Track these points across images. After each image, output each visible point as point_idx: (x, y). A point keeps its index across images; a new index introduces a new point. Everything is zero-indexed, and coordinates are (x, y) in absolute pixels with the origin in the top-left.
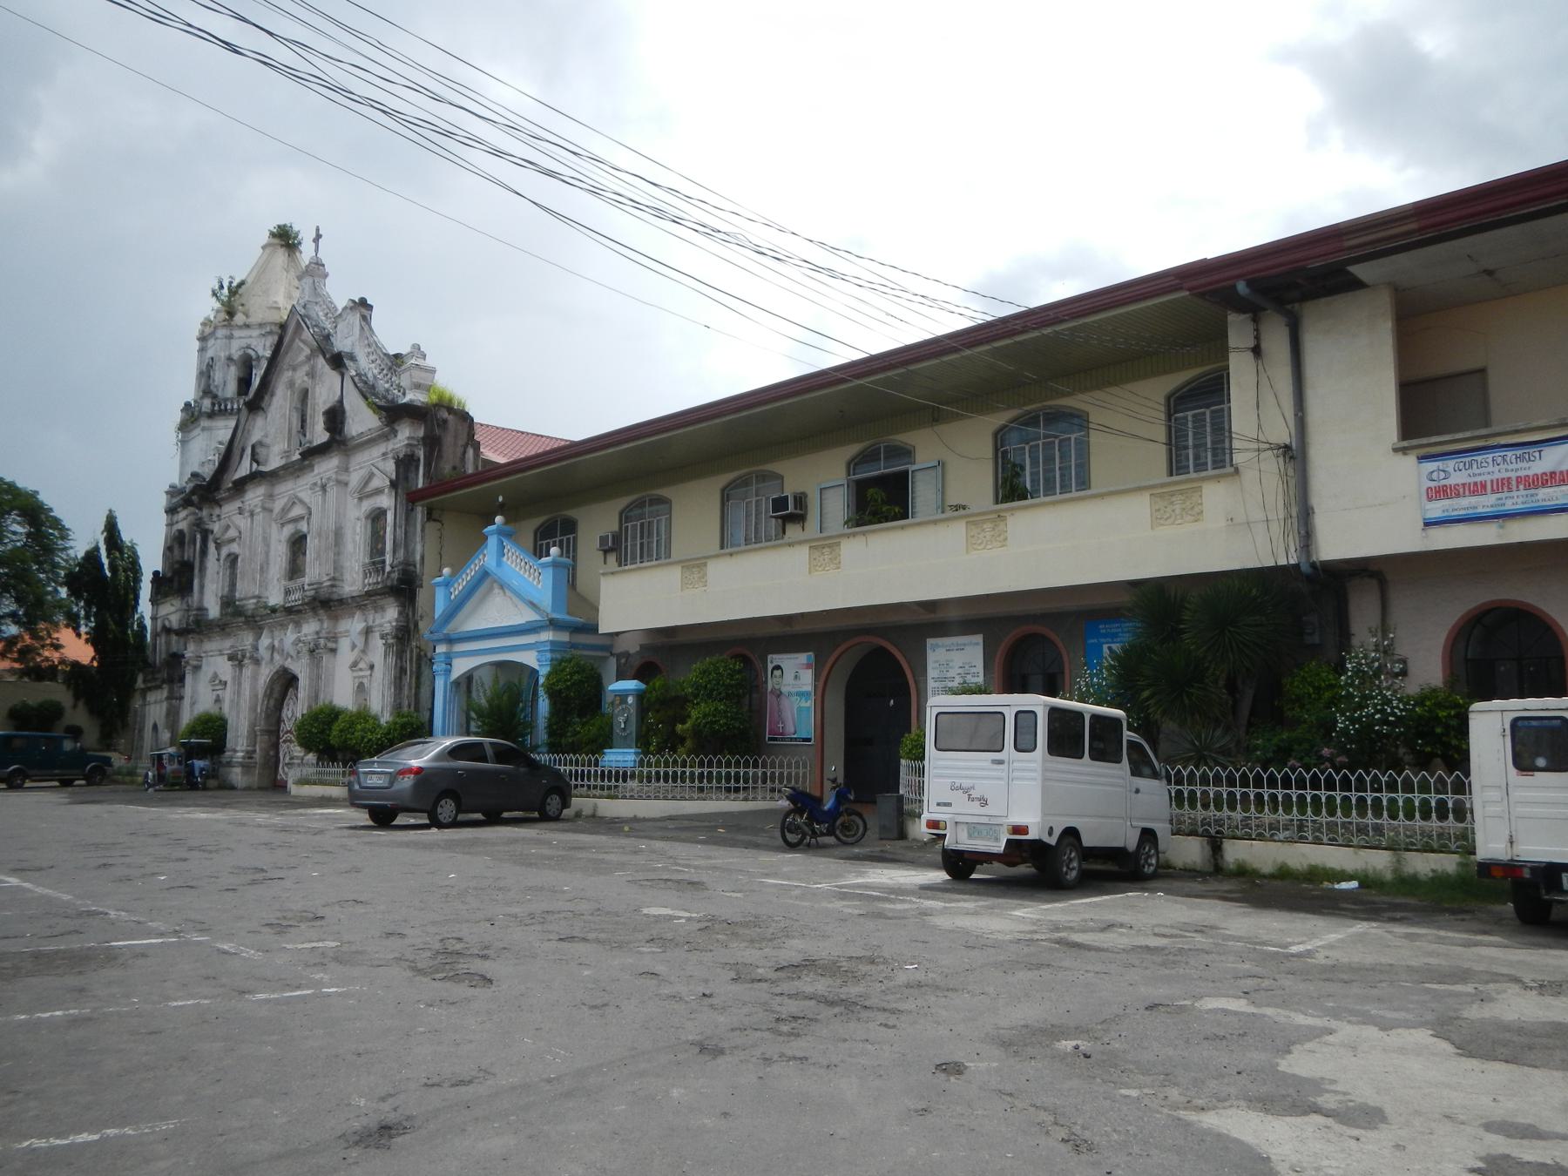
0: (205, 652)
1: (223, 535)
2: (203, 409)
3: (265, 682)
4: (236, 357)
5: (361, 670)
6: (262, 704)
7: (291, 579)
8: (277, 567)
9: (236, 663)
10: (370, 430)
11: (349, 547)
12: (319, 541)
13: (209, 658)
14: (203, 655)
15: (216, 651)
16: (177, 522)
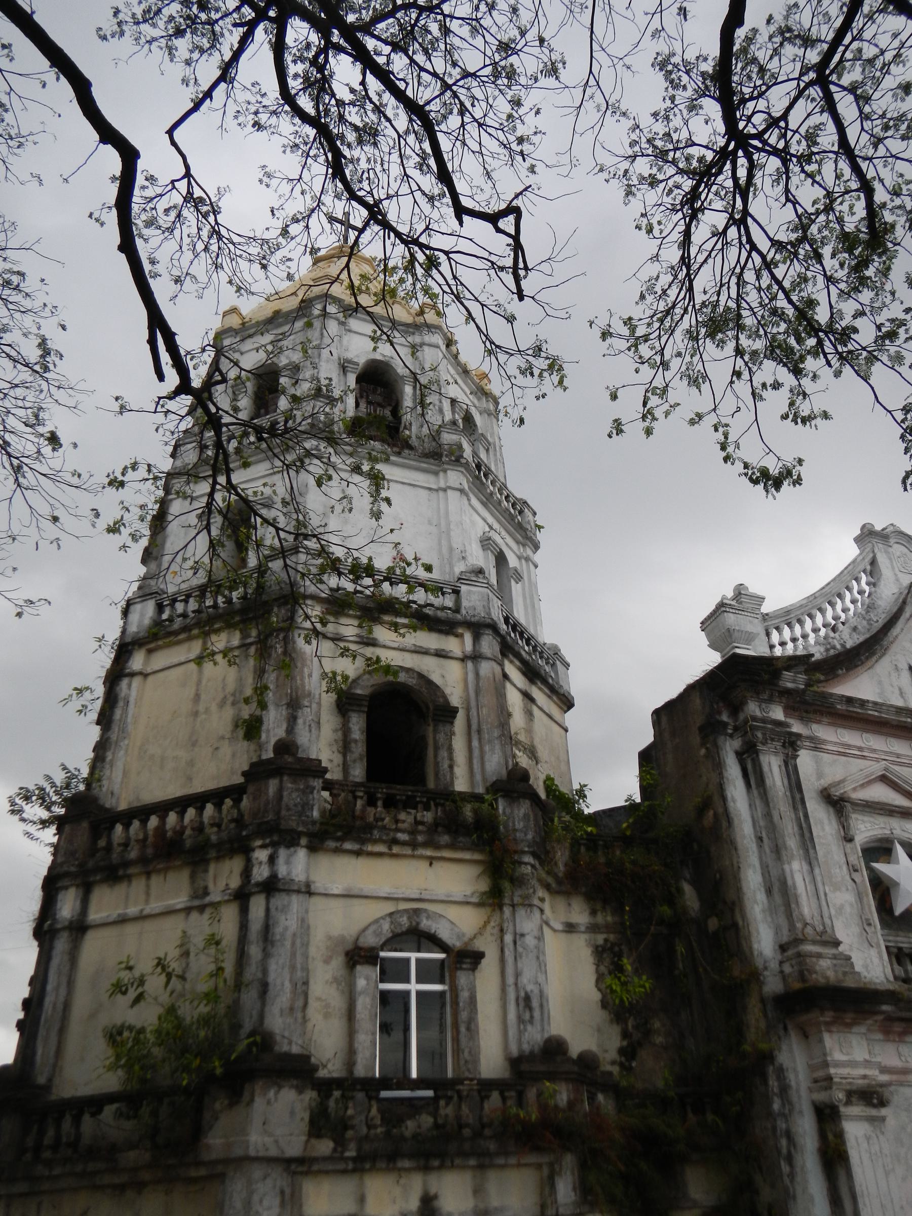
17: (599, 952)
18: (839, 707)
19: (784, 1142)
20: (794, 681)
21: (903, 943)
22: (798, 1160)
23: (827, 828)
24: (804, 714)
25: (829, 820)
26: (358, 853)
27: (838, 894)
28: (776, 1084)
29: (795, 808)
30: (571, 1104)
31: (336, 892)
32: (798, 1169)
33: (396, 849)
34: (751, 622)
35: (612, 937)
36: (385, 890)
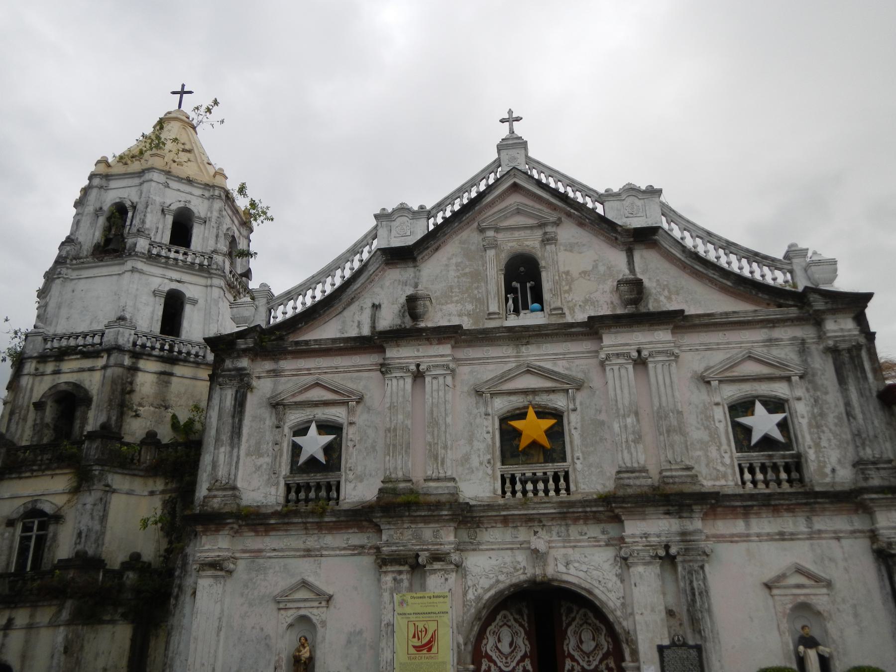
0: (244, 551)
1: (294, 395)
2: (138, 249)
3: (479, 598)
4: (174, 207)
5: (799, 586)
6: (471, 630)
7: (503, 464)
8: (479, 445)
9: (406, 568)
10: (756, 311)
11: (697, 434)
12: (638, 421)
13: (261, 561)
14: (238, 555)
15: (297, 550)
16: (57, 372)
17: (165, 503)
18: (290, 349)
19: (176, 590)
20: (246, 343)
21: (289, 481)
22: (182, 598)
23: (268, 422)
24: (274, 357)
25: (271, 417)
26: (20, 478)
27: (261, 459)
28: (180, 562)
29: (233, 417)
30: (73, 578)
31: (6, 497)
32: (180, 602)
33: (35, 474)
34: (247, 310)
35: (174, 495)
36: (26, 493)
